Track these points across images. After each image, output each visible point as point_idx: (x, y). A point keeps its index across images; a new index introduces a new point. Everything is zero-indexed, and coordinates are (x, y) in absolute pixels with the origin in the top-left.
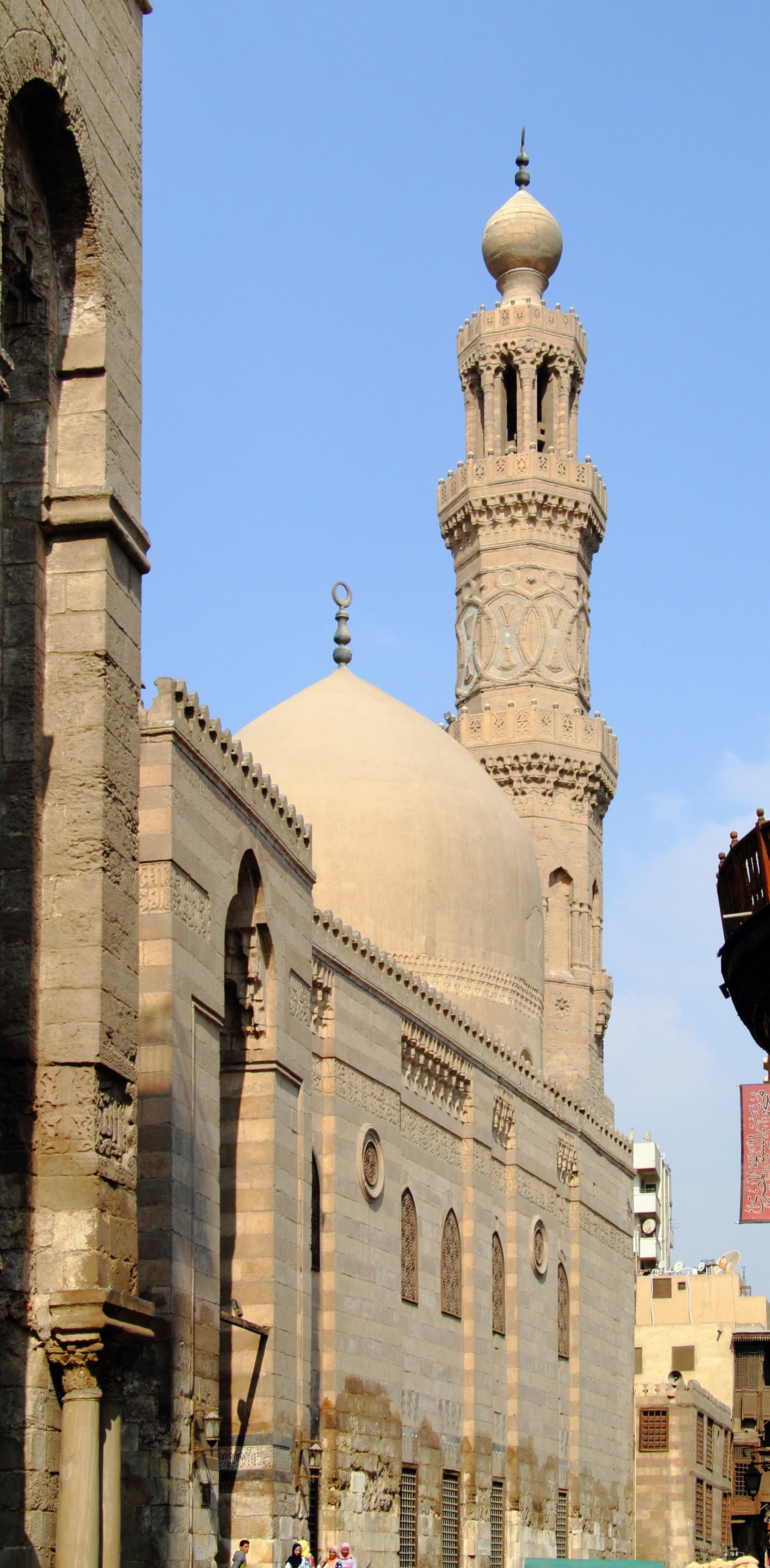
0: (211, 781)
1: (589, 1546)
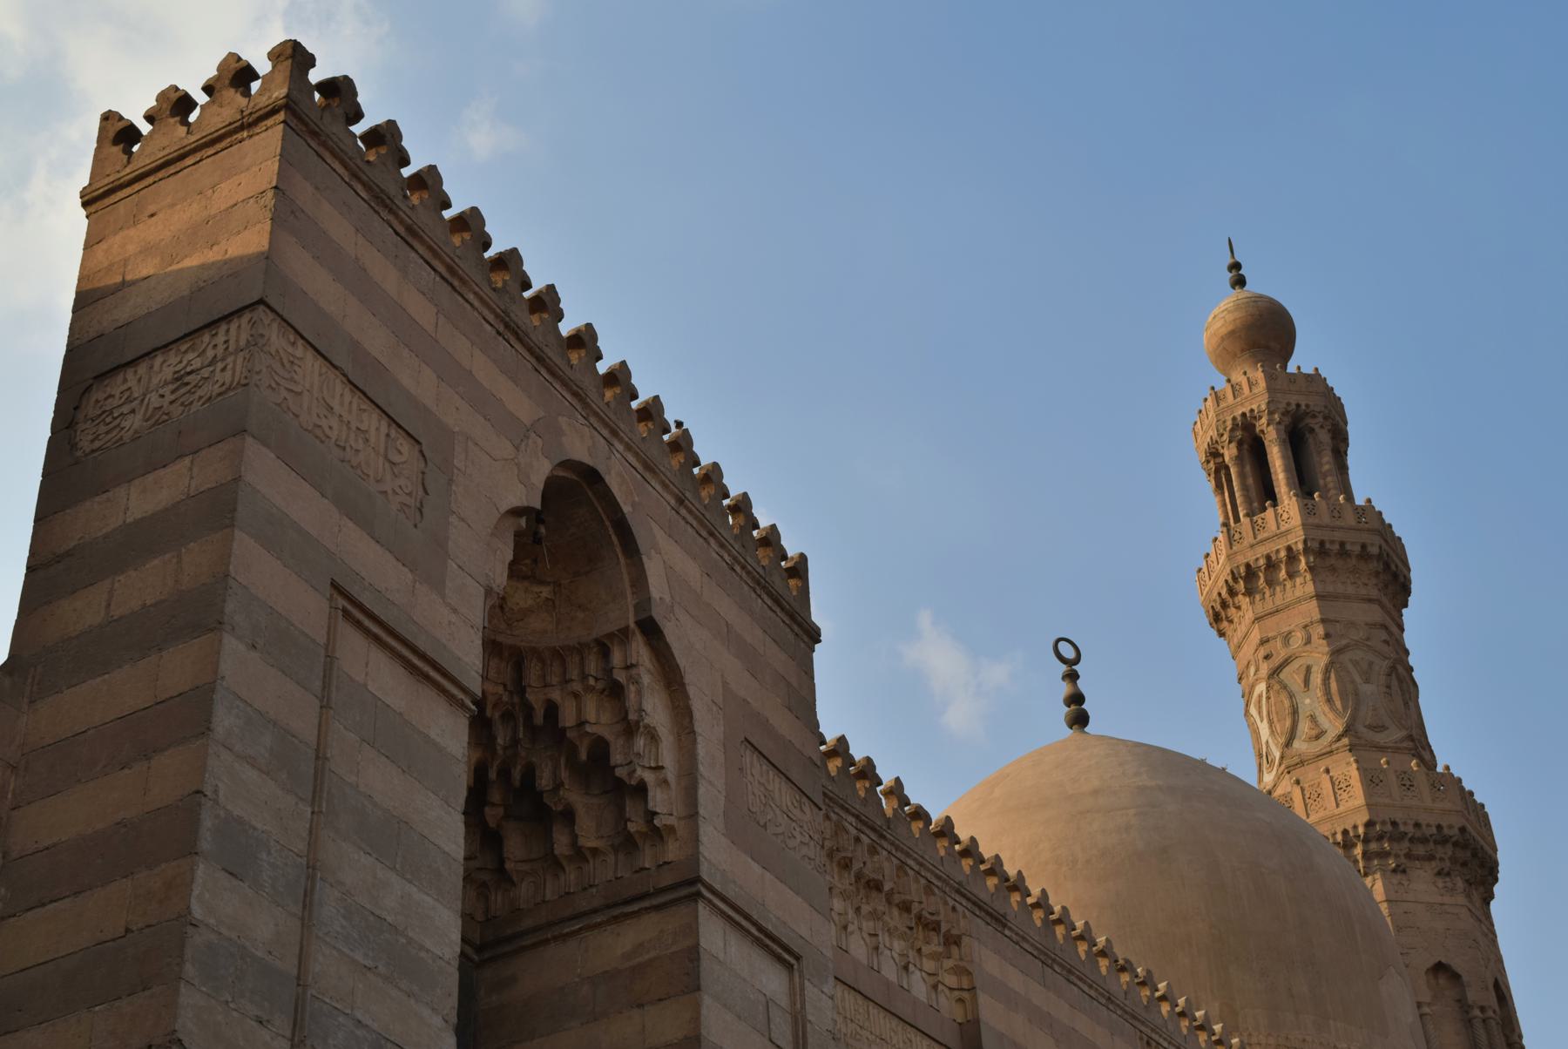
0: (443, 277)
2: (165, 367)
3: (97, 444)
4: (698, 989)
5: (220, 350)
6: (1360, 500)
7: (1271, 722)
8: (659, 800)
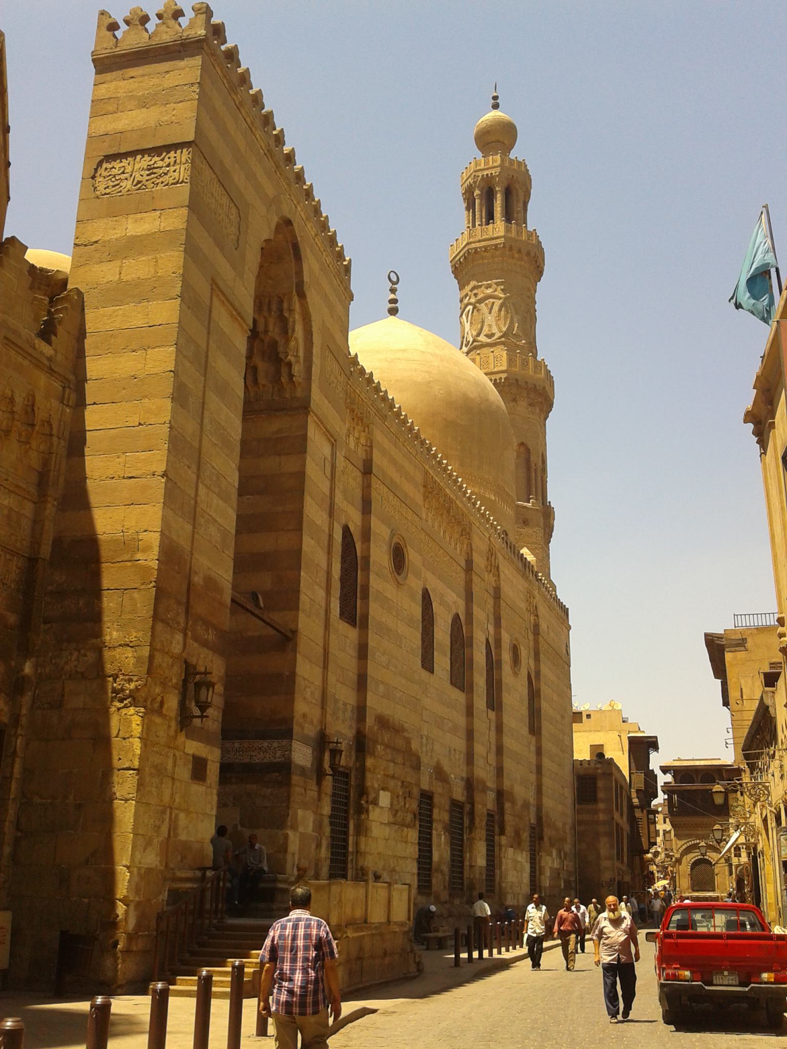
1: (550, 865)
2: (144, 162)
3: (108, 191)
4: (306, 452)
5: (173, 160)
6: (530, 229)
7: (471, 323)
8: (297, 369)
